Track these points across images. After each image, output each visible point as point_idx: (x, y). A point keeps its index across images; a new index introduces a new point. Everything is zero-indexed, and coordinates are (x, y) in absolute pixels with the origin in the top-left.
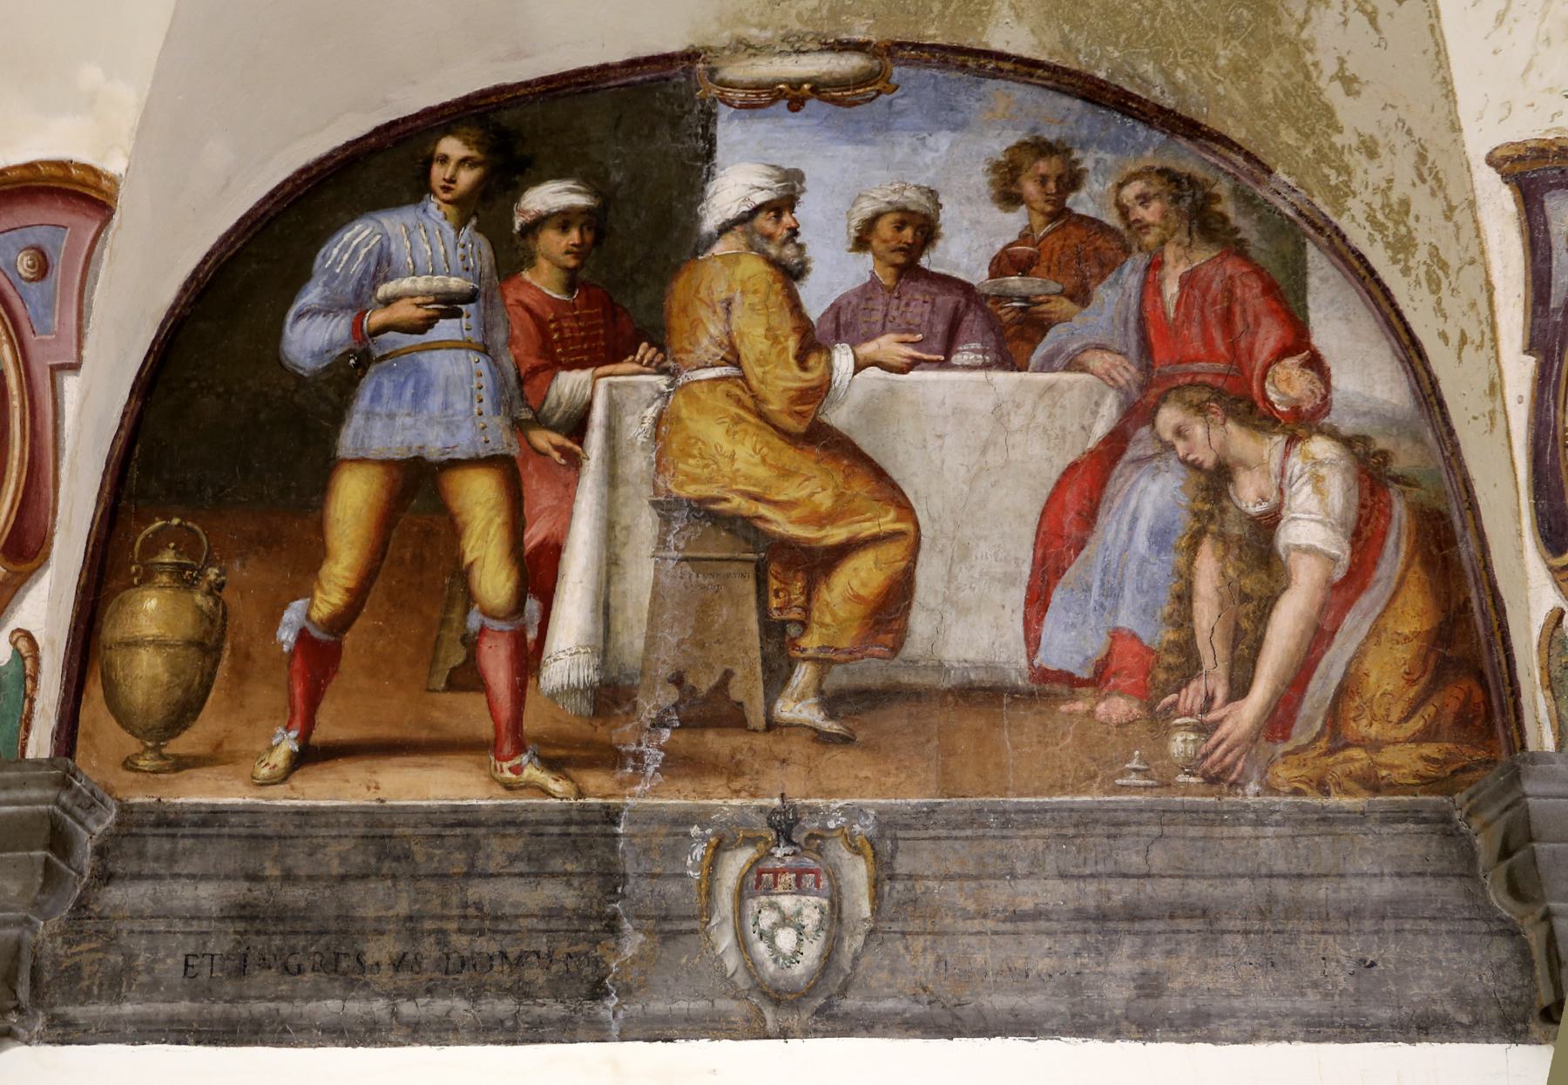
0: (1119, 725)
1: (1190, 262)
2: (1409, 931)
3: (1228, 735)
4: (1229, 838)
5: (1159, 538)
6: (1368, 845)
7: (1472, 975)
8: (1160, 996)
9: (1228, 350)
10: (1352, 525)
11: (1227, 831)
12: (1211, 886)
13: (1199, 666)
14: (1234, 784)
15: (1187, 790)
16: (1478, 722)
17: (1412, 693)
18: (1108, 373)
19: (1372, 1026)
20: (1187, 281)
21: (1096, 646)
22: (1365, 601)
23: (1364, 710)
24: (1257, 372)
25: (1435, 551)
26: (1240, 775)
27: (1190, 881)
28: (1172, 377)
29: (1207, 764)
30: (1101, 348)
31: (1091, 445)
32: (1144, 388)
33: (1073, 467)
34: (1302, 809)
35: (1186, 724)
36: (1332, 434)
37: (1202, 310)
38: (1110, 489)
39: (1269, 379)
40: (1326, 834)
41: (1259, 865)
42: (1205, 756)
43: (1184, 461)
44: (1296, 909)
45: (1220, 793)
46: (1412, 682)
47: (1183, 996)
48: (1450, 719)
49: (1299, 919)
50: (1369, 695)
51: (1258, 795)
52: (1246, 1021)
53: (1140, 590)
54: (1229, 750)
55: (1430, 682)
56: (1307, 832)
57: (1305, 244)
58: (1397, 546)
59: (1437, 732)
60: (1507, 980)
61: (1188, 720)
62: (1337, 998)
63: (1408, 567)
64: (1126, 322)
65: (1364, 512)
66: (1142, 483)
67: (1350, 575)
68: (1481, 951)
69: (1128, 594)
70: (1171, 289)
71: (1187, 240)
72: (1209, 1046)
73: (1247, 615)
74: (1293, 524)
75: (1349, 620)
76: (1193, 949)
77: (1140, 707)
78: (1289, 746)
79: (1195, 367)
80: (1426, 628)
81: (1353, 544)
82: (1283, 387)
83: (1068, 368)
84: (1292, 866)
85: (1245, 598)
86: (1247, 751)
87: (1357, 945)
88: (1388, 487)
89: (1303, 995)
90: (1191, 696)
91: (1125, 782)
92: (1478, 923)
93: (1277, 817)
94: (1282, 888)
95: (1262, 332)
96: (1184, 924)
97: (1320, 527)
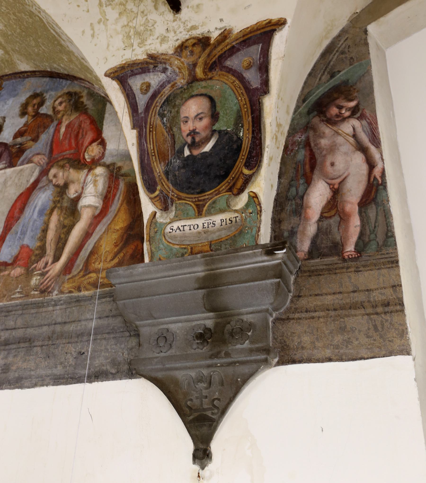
0: (16, 277)
1: (70, 119)
2: (99, 339)
3: (50, 275)
4: (44, 312)
5: (41, 213)
6: (91, 308)
7: (120, 353)
8: (8, 372)
9: (75, 145)
10: (104, 194)
11: (44, 309)
12: (34, 330)
13: (45, 253)
14: (50, 292)
15: (34, 296)
16: (138, 256)
17: (116, 250)
18: (38, 162)
19: (78, 378)
20: (68, 126)
21: (15, 251)
22: (105, 220)
23: (98, 259)
24: (83, 150)
25: (132, 197)
26: (52, 289)
27: (28, 329)
28: (57, 158)
29: (41, 286)
30: (38, 154)
31: (28, 186)
32: (48, 164)
33: (22, 193)
34: (71, 298)
35: (38, 274)
36: (104, 165)
37: (70, 135)
38: (30, 199)
39: (87, 151)
40: (77, 306)
41: (52, 320)
42: (42, 284)
43: (54, 185)
44: (61, 335)
45: (45, 296)
46: (116, 246)
47: (15, 372)
48: (128, 257)
49: (61, 339)
50: (100, 253)
51: (57, 295)
52: (34, 380)
53: (32, 231)
54: (50, 280)
55: (123, 245)
56: (71, 306)
57: (106, 104)
58: (119, 199)
59: (123, 262)
60: (133, 354)
61: (39, 272)
62: (68, 368)
63: (121, 205)
64: (47, 144)
65: (110, 189)
66: (40, 195)
67: (101, 212)
68: (124, 344)
69: (28, 233)
70: (63, 130)
71: (70, 113)
72: (20, 390)
73: (63, 233)
74: (85, 198)
75: (98, 228)
76: (23, 354)
77: (24, 270)
78: (70, 276)
79: (64, 153)
80: (125, 225)
81: (104, 201)
82: (90, 153)
83: (27, 163)
84: (63, 319)
85: (64, 227)
86: (56, 280)
87: (80, 346)
88: (119, 178)
89: (56, 367)
90: (41, 264)
91: (14, 296)
92: (125, 333)
93: (62, 302)
94: (58, 328)
95: (87, 137)
96: (22, 345)
97: (94, 197)
